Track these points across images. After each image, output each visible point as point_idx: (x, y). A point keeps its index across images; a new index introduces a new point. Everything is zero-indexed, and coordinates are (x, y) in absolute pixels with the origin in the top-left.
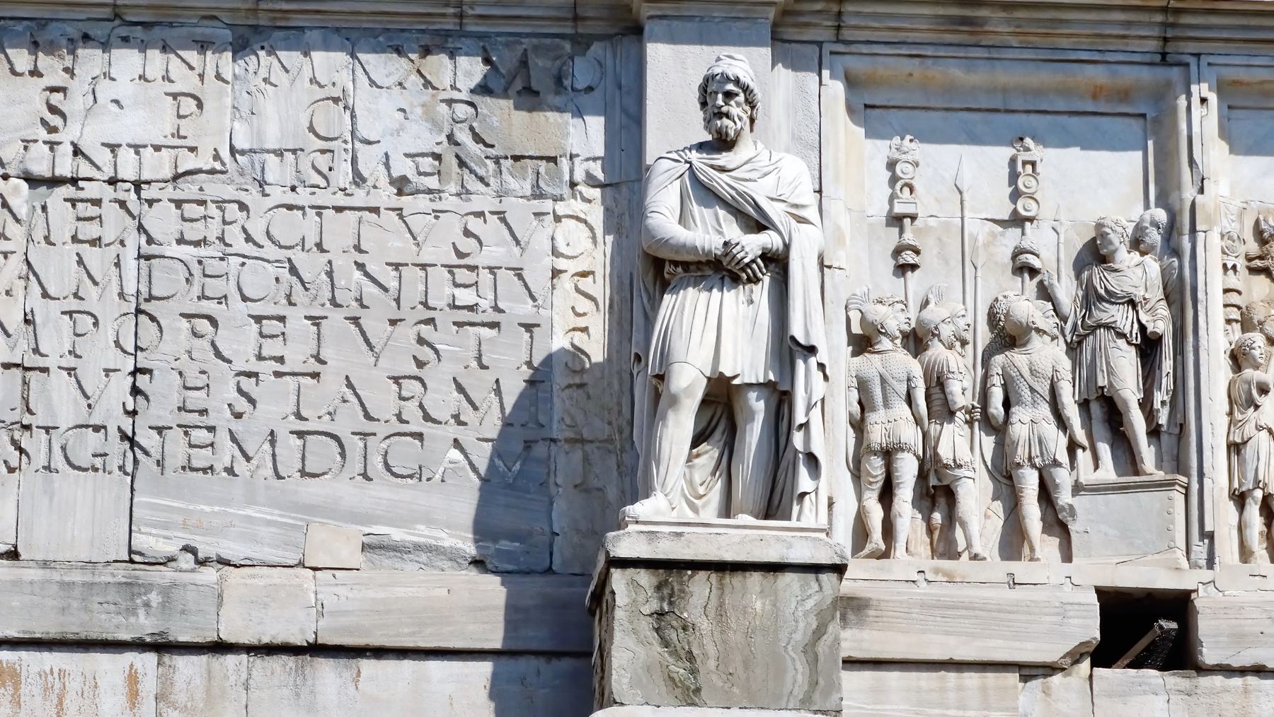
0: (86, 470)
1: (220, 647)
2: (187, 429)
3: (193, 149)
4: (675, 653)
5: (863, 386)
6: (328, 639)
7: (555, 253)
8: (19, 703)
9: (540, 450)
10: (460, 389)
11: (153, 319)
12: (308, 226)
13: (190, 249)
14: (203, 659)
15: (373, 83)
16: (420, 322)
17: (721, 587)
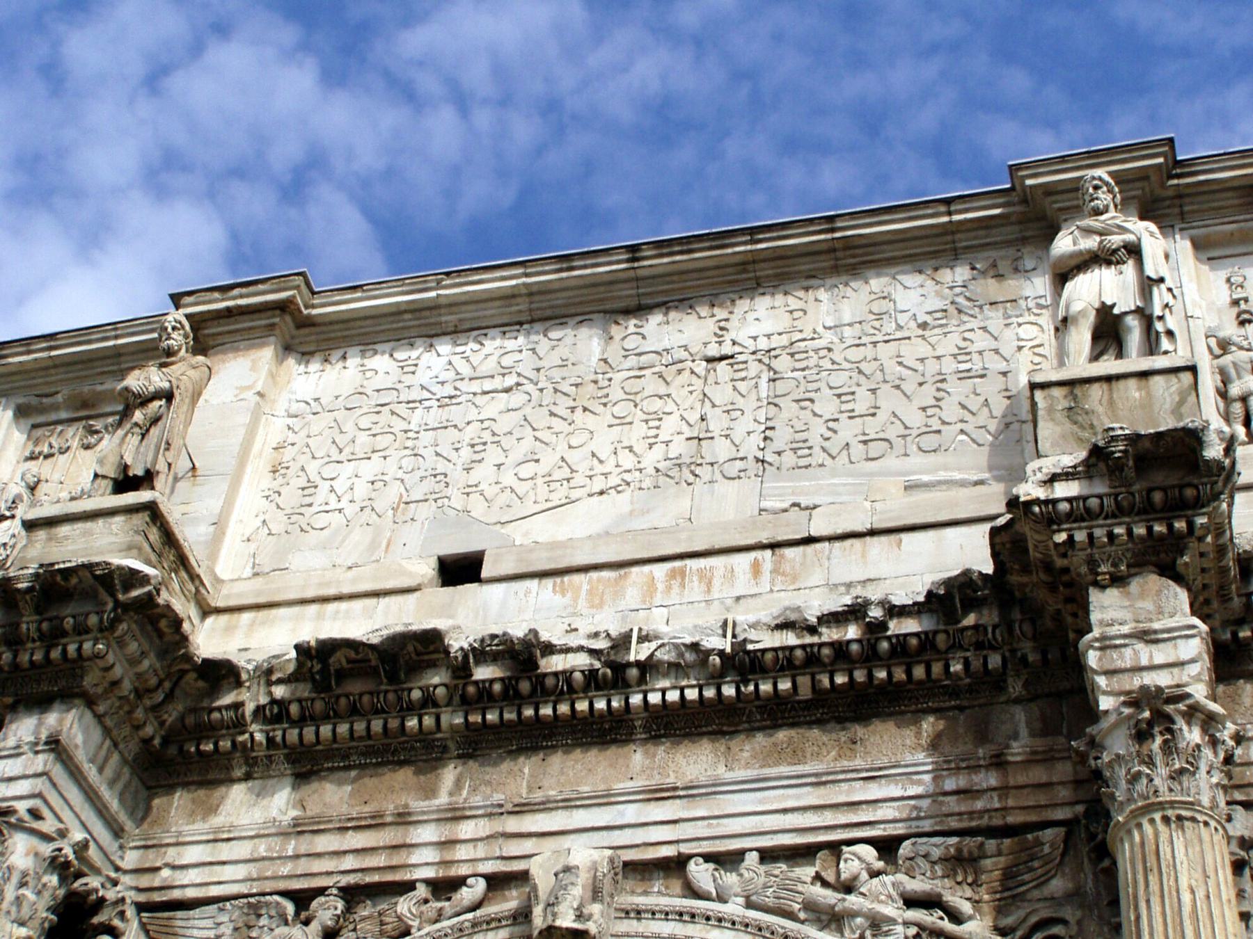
0: (733, 479)
1: (809, 540)
2: (794, 450)
3: (801, 331)
4: (1082, 427)
5: (1223, 372)
6: (877, 525)
7: (1019, 339)
8: (684, 587)
9: (1015, 426)
10: (964, 407)
11: (776, 405)
12: (868, 352)
13: (800, 373)
14: (801, 549)
15: (905, 287)
16: (937, 382)
17: (1111, 390)
